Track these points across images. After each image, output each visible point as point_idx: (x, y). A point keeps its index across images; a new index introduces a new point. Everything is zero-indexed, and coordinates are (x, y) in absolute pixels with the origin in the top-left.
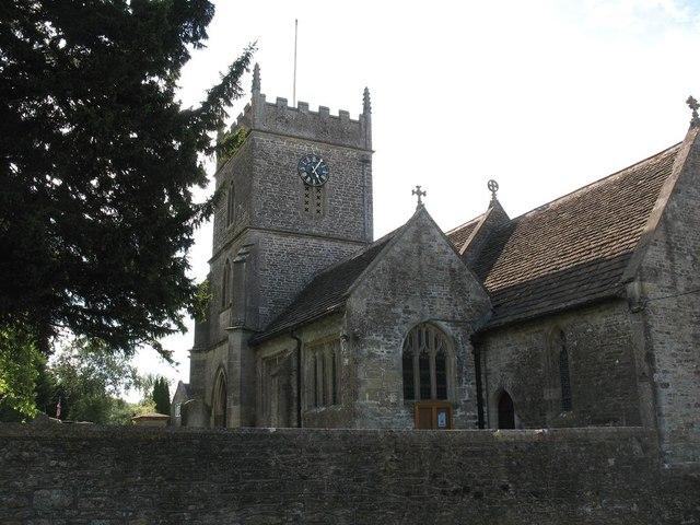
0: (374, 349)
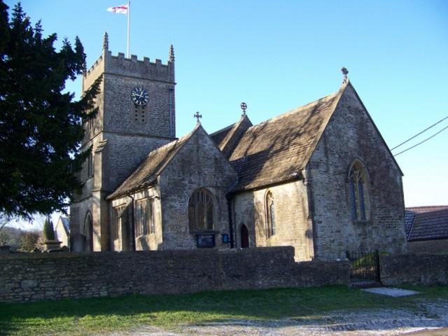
0: (172, 204)
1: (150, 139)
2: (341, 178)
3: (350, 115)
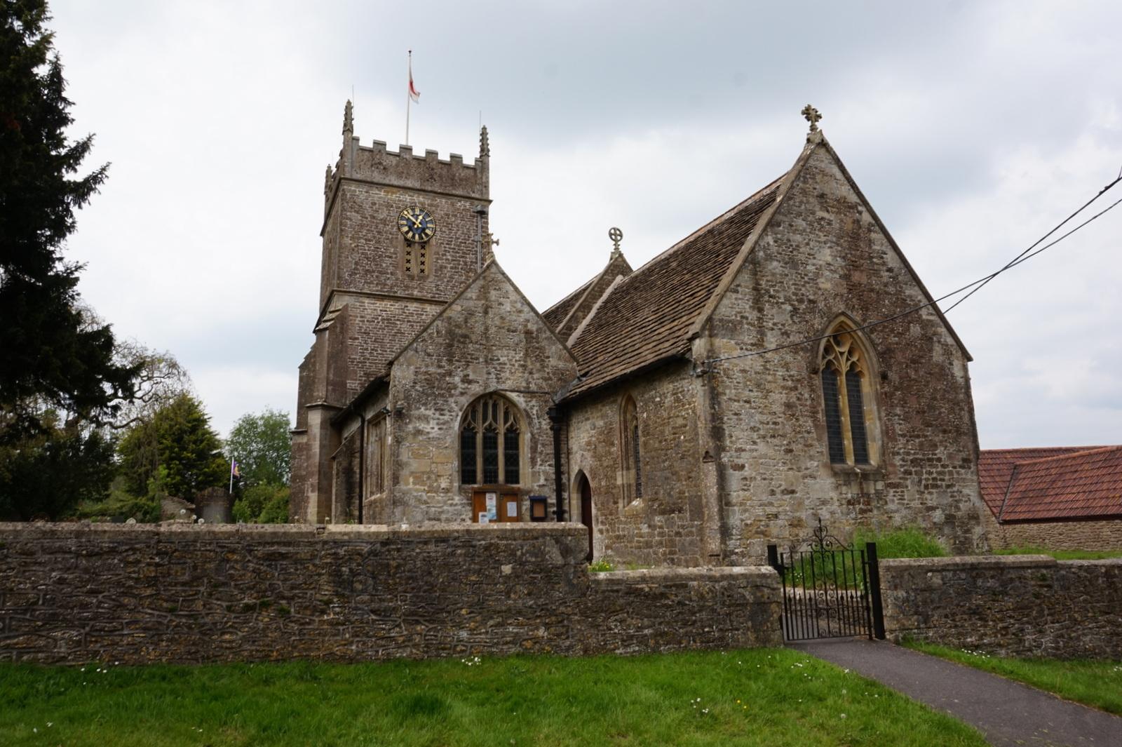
0: (422, 426)
1: (433, 307)
2: (799, 364)
3: (825, 215)
